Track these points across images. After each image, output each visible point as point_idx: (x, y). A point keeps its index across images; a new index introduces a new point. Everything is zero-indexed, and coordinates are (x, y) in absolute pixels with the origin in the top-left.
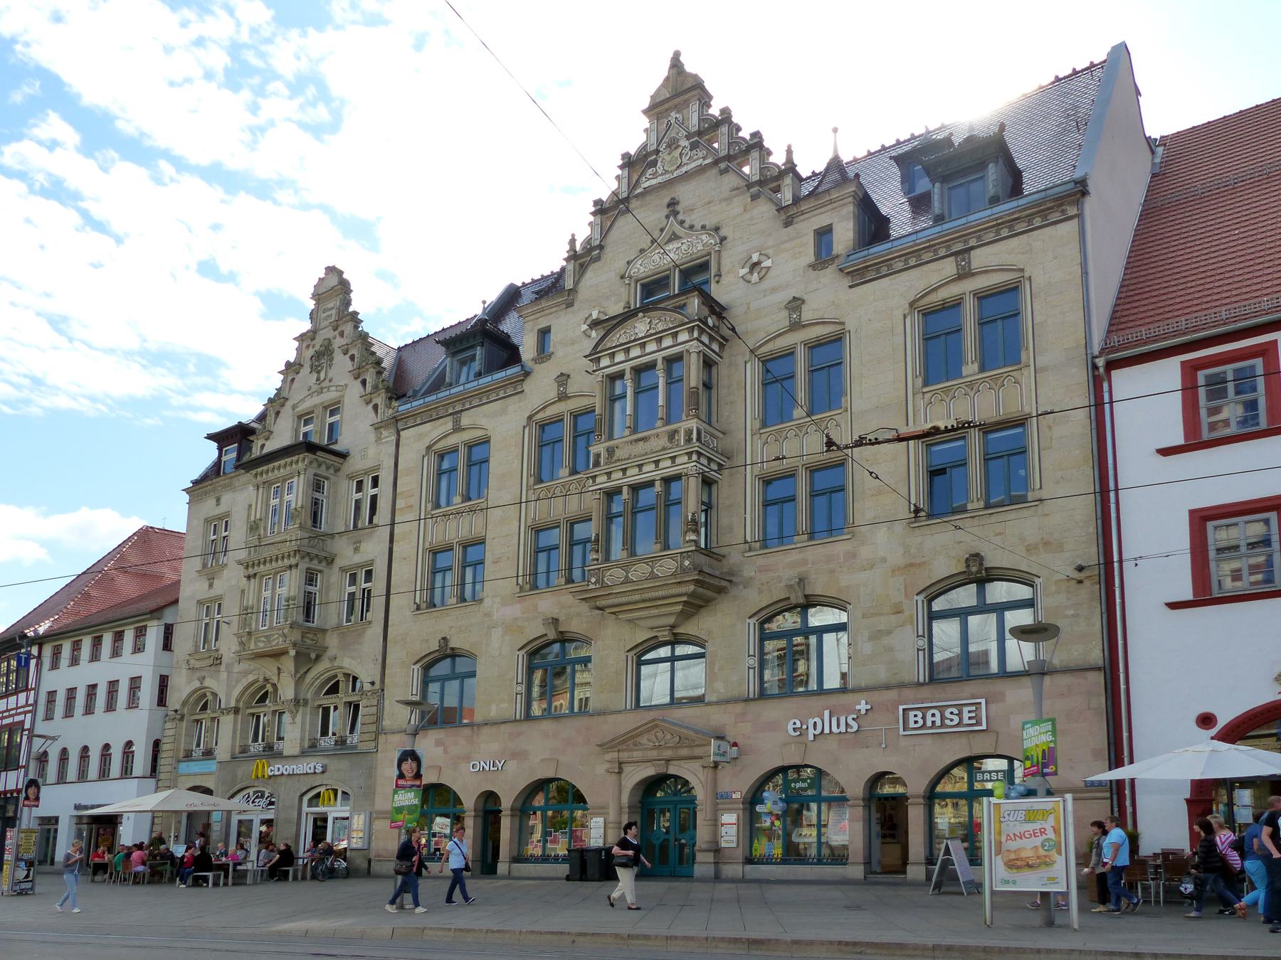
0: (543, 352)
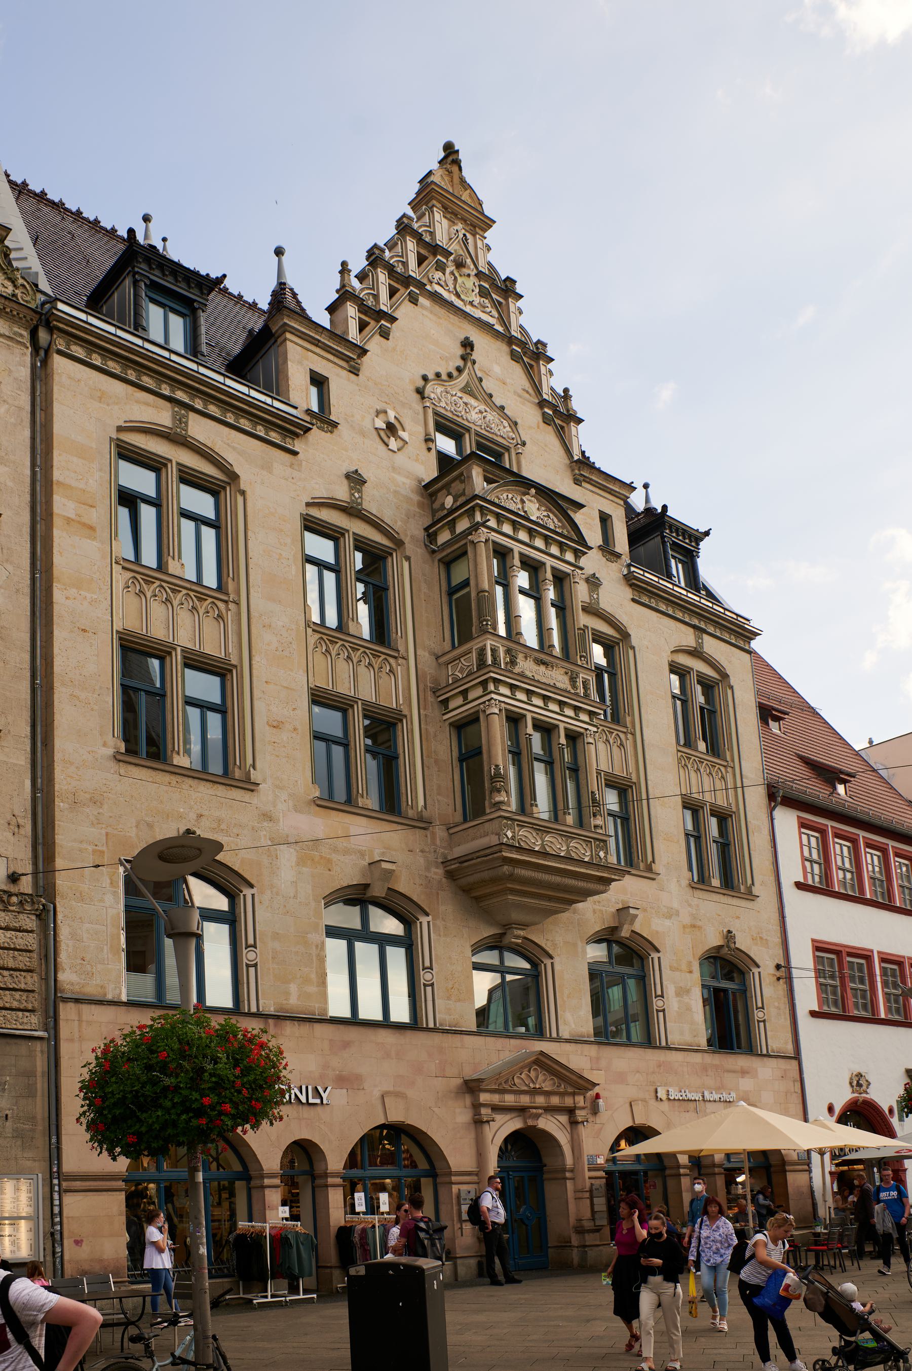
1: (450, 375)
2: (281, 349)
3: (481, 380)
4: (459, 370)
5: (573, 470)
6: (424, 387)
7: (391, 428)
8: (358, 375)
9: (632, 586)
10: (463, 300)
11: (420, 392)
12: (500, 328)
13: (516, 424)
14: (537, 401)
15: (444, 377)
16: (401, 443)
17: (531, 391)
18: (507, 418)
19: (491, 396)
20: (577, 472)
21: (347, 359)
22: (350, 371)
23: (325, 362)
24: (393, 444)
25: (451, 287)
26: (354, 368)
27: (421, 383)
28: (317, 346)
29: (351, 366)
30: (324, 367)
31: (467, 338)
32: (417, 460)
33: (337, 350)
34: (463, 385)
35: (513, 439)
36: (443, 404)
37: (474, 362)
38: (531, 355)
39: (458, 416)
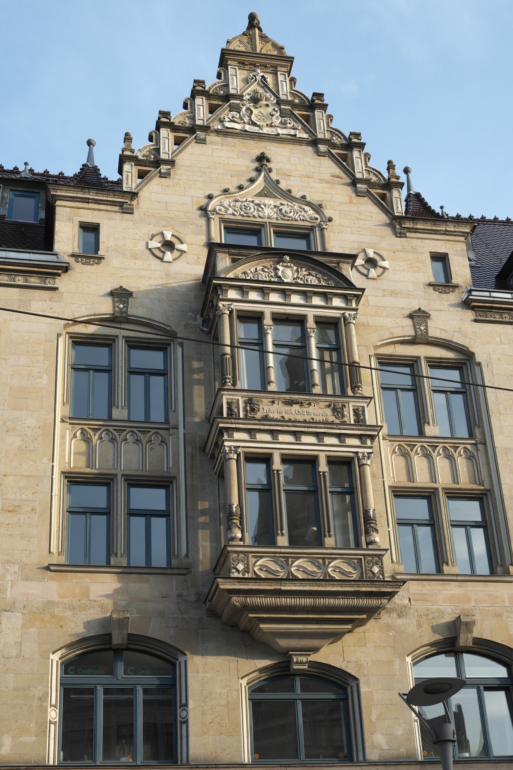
1: (241, 188)
3: (278, 182)
4: (252, 181)
5: (394, 229)
6: (208, 205)
7: (169, 245)
8: (132, 213)
9: (473, 308)
10: (259, 126)
11: (203, 209)
12: (305, 136)
13: (320, 206)
14: (351, 181)
15: (232, 190)
17: (342, 174)
18: (309, 204)
19: (289, 191)
20: (398, 227)
21: (121, 205)
22: (123, 213)
23: (96, 212)
24: (169, 256)
25: (246, 119)
26: (128, 209)
28: (88, 203)
29: (122, 209)
30: (89, 216)
31: (263, 153)
33: (108, 201)
35: (317, 219)
36: (231, 211)
37: (270, 170)
38: (345, 148)
39: (249, 217)
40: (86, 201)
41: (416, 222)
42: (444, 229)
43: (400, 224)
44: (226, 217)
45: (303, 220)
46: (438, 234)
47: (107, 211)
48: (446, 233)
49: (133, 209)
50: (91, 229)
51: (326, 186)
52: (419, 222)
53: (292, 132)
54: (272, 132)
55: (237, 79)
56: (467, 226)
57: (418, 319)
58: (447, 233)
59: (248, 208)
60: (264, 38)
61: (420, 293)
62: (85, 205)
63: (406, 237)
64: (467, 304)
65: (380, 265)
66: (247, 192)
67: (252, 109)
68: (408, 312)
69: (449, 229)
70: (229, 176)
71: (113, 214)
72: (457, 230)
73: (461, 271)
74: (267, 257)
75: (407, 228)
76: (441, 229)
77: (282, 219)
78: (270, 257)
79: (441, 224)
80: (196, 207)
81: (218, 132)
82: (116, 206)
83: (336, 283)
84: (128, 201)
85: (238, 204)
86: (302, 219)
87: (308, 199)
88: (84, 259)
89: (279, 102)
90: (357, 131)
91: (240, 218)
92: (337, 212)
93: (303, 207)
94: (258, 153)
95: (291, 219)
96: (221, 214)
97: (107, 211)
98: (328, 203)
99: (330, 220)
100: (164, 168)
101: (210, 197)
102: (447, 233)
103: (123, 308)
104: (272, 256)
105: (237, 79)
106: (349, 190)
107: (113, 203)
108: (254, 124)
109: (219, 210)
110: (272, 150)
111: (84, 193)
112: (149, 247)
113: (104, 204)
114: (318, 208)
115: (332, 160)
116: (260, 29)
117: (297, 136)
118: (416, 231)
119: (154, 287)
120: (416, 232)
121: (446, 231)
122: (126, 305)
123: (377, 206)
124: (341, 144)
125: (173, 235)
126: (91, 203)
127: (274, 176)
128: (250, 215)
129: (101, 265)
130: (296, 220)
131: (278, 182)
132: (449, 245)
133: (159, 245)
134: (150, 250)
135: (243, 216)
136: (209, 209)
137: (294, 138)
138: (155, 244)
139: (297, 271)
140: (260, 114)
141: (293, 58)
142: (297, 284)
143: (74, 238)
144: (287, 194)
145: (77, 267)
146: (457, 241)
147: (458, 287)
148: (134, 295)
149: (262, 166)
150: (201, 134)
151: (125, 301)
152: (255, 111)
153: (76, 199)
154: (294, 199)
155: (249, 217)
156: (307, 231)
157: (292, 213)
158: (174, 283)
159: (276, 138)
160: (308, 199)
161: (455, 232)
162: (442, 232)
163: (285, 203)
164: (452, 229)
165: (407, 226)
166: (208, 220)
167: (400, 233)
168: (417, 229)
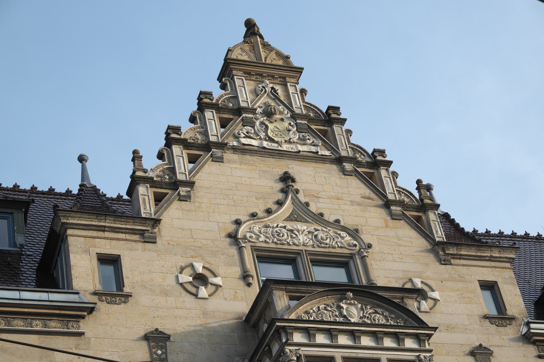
0: (116, 290)
1: (269, 212)
2: (66, 244)
3: (307, 204)
4: (280, 204)
5: (437, 255)
6: (237, 231)
7: (201, 279)
8: (155, 243)
9: (534, 343)
10: (277, 142)
11: (233, 237)
12: (327, 153)
13: (357, 231)
14: (384, 203)
15: (260, 214)
16: (214, 288)
17: (373, 195)
18: (344, 229)
19: (322, 215)
20: (441, 253)
21: (142, 233)
22: (145, 242)
23: (114, 242)
24: (203, 292)
25: (262, 135)
26: (150, 237)
27: (233, 227)
28: (104, 231)
30: (109, 248)
31: (286, 173)
32: (235, 298)
34: (288, 214)
35: (355, 245)
36: (262, 238)
37: (297, 191)
38: (372, 167)
39: (283, 244)
40: (102, 229)
41: (460, 247)
42: (489, 255)
43: (444, 250)
44: (258, 244)
45: (341, 247)
46: (483, 260)
47: (127, 240)
48: (491, 259)
49: (155, 238)
50: (110, 261)
51: (358, 208)
52: (463, 248)
53: (313, 149)
54: (292, 148)
55: (245, 90)
56: (513, 251)
57: (481, 357)
58: (492, 259)
59: (281, 235)
60: (266, 46)
61: (476, 327)
62: (101, 234)
63: (451, 264)
64: (528, 338)
65: (431, 296)
66: (276, 217)
67: (267, 123)
68: (468, 349)
69: (494, 255)
70: (254, 199)
71: (133, 244)
72: (502, 256)
73: (515, 302)
74: (329, 294)
75: (451, 254)
76: (486, 255)
77: (319, 247)
78: (332, 294)
79: (486, 249)
80: (223, 234)
81: (234, 149)
82: (136, 234)
83: (405, 321)
84: (149, 228)
85: (270, 230)
86: (340, 245)
87: (342, 224)
88: (109, 298)
89: (294, 116)
90: (381, 147)
91: (273, 246)
92: (375, 237)
93: (339, 232)
94: (280, 172)
95: (328, 246)
96: (252, 242)
97: (127, 240)
98: (363, 227)
99: (370, 246)
100: (183, 190)
101: (238, 223)
102: (492, 259)
103: (162, 354)
104: (334, 293)
105: (245, 90)
106: (383, 212)
107: (133, 232)
108: (271, 140)
109: (250, 237)
110: (295, 169)
111: (100, 220)
112: (181, 282)
113: (122, 233)
114: (354, 233)
115: (360, 180)
116: (261, 37)
117: (319, 153)
118: (460, 257)
119: (192, 328)
120: (460, 259)
121: (491, 257)
122: (164, 350)
123: (415, 230)
124: (367, 162)
125: (204, 267)
126: (107, 231)
127: (302, 198)
128: (284, 242)
129: (129, 304)
130: (334, 247)
131: (307, 204)
132: (497, 272)
133: (191, 279)
134: (181, 284)
135: (276, 243)
136: (239, 236)
137: (315, 155)
138: (185, 278)
139: (362, 309)
140: (276, 129)
141: (303, 69)
142: (364, 324)
143: (93, 272)
144: (319, 218)
145: (103, 307)
146: (503, 268)
147: (514, 319)
148: (171, 339)
149: (288, 187)
150: (217, 152)
151: (162, 346)
152: (271, 126)
153: (90, 228)
154: (327, 224)
155: (283, 244)
156: (346, 260)
157: (328, 240)
158: (214, 323)
159: (297, 156)
160: (342, 224)
161: (500, 257)
162: (487, 258)
163: (320, 228)
164: (497, 255)
165: (451, 252)
166: (240, 249)
167: (444, 260)
168: (461, 255)
